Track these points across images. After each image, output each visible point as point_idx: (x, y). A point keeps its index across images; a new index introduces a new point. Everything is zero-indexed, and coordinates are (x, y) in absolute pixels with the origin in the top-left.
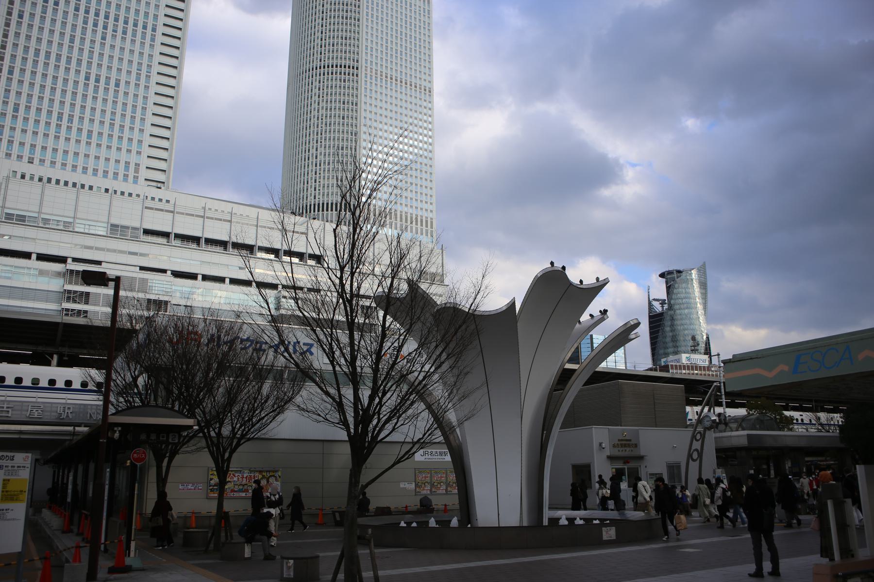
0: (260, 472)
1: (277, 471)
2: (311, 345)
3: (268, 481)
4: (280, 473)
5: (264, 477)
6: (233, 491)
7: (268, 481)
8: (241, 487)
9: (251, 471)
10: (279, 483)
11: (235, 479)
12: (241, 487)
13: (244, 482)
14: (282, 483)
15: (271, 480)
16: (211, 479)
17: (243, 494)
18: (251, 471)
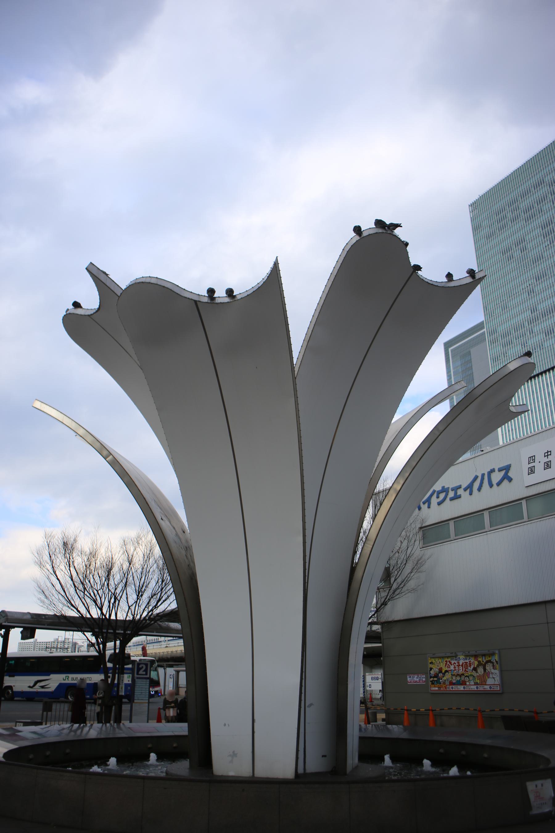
0: (476, 656)
1: (493, 654)
2: (507, 468)
3: (485, 670)
4: (496, 657)
5: (480, 664)
6: (451, 683)
7: (485, 670)
8: (458, 678)
9: (466, 656)
10: (497, 672)
11: (452, 668)
12: (458, 678)
13: (461, 672)
14: (501, 671)
15: (489, 667)
16: (431, 669)
17: (461, 688)
18: (466, 656)
